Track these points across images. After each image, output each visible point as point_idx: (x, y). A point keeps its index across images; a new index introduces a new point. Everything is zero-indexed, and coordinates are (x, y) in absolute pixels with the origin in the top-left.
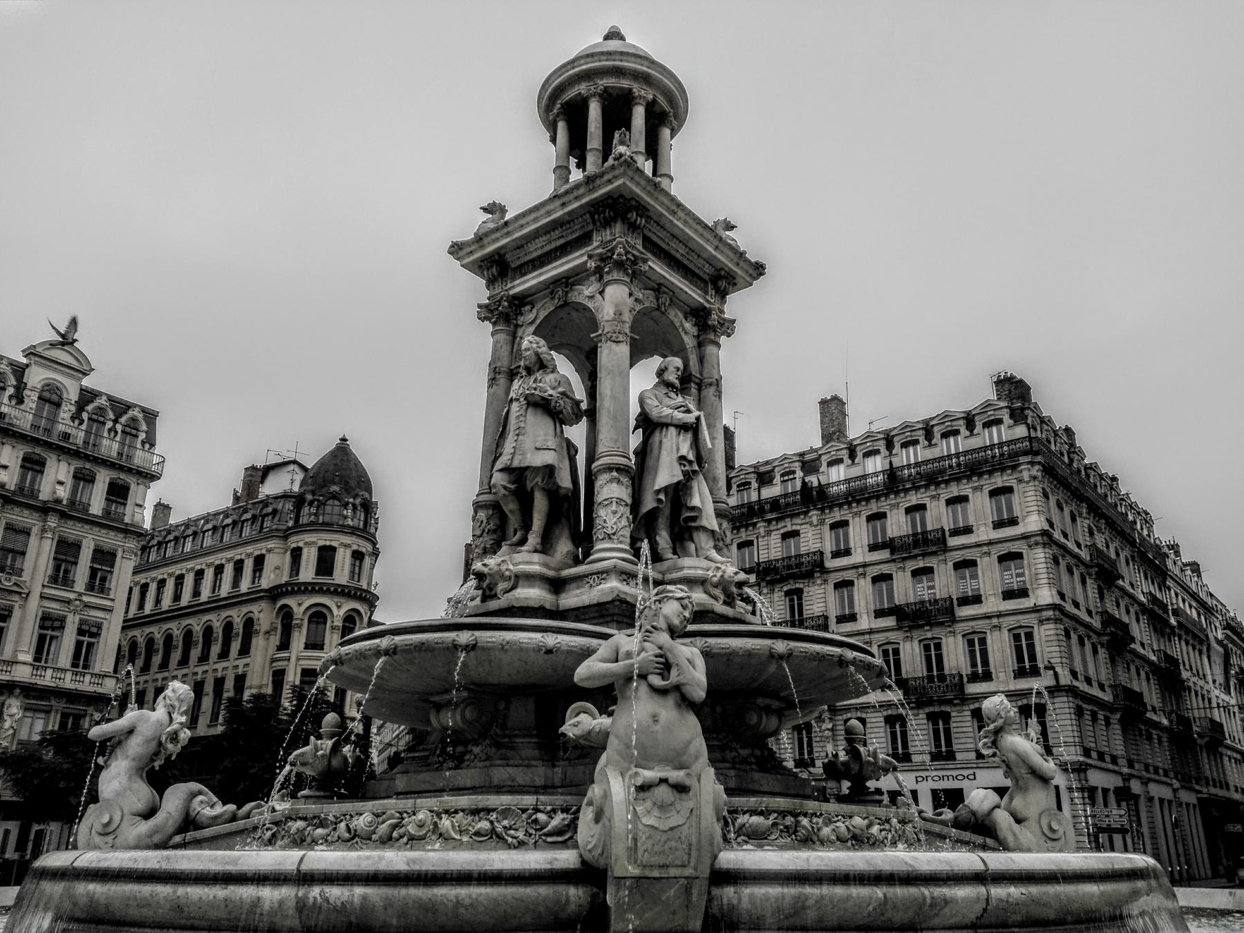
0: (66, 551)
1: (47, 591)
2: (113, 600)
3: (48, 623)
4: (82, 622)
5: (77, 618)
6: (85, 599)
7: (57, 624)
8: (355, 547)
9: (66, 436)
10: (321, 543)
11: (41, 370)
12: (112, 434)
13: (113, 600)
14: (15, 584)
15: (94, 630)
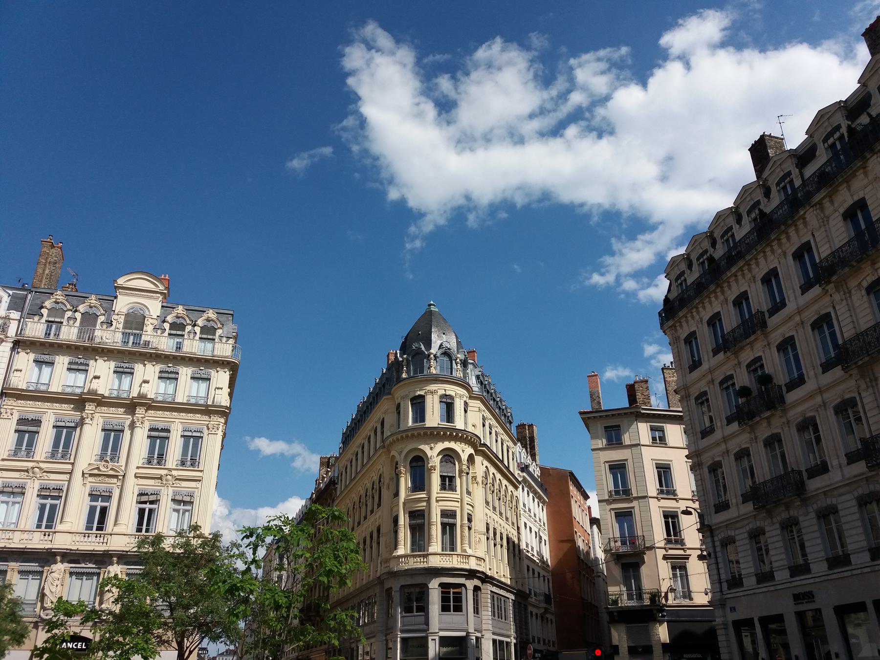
0: (159, 437)
1: (141, 471)
2: (201, 471)
3: (144, 498)
4: (175, 493)
5: (171, 490)
6: (174, 473)
7: (152, 498)
8: (441, 392)
9: (147, 343)
10: (412, 396)
11: (126, 298)
12: (192, 336)
13: (201, 471)
14: (112, 469)
15: (187, 499)
